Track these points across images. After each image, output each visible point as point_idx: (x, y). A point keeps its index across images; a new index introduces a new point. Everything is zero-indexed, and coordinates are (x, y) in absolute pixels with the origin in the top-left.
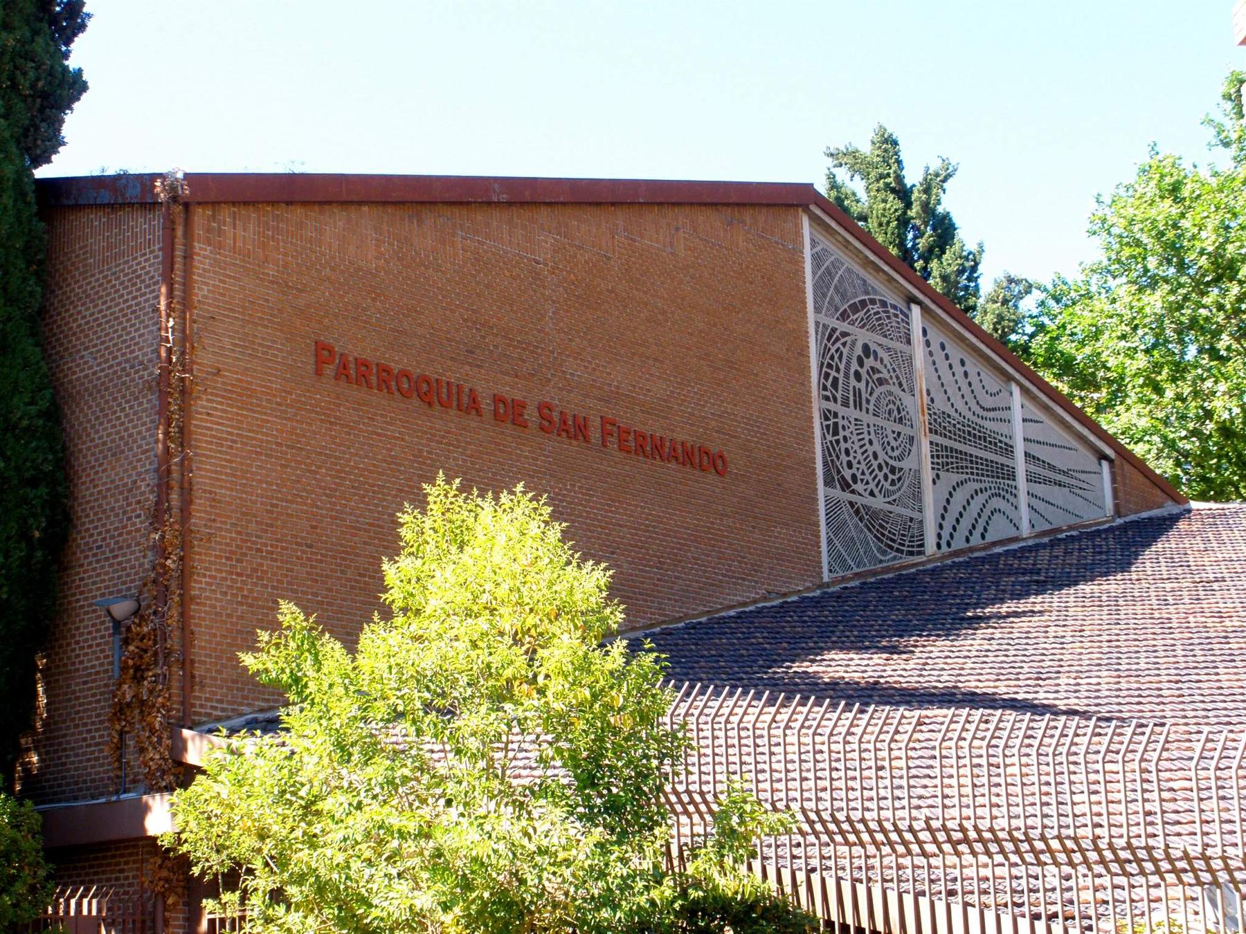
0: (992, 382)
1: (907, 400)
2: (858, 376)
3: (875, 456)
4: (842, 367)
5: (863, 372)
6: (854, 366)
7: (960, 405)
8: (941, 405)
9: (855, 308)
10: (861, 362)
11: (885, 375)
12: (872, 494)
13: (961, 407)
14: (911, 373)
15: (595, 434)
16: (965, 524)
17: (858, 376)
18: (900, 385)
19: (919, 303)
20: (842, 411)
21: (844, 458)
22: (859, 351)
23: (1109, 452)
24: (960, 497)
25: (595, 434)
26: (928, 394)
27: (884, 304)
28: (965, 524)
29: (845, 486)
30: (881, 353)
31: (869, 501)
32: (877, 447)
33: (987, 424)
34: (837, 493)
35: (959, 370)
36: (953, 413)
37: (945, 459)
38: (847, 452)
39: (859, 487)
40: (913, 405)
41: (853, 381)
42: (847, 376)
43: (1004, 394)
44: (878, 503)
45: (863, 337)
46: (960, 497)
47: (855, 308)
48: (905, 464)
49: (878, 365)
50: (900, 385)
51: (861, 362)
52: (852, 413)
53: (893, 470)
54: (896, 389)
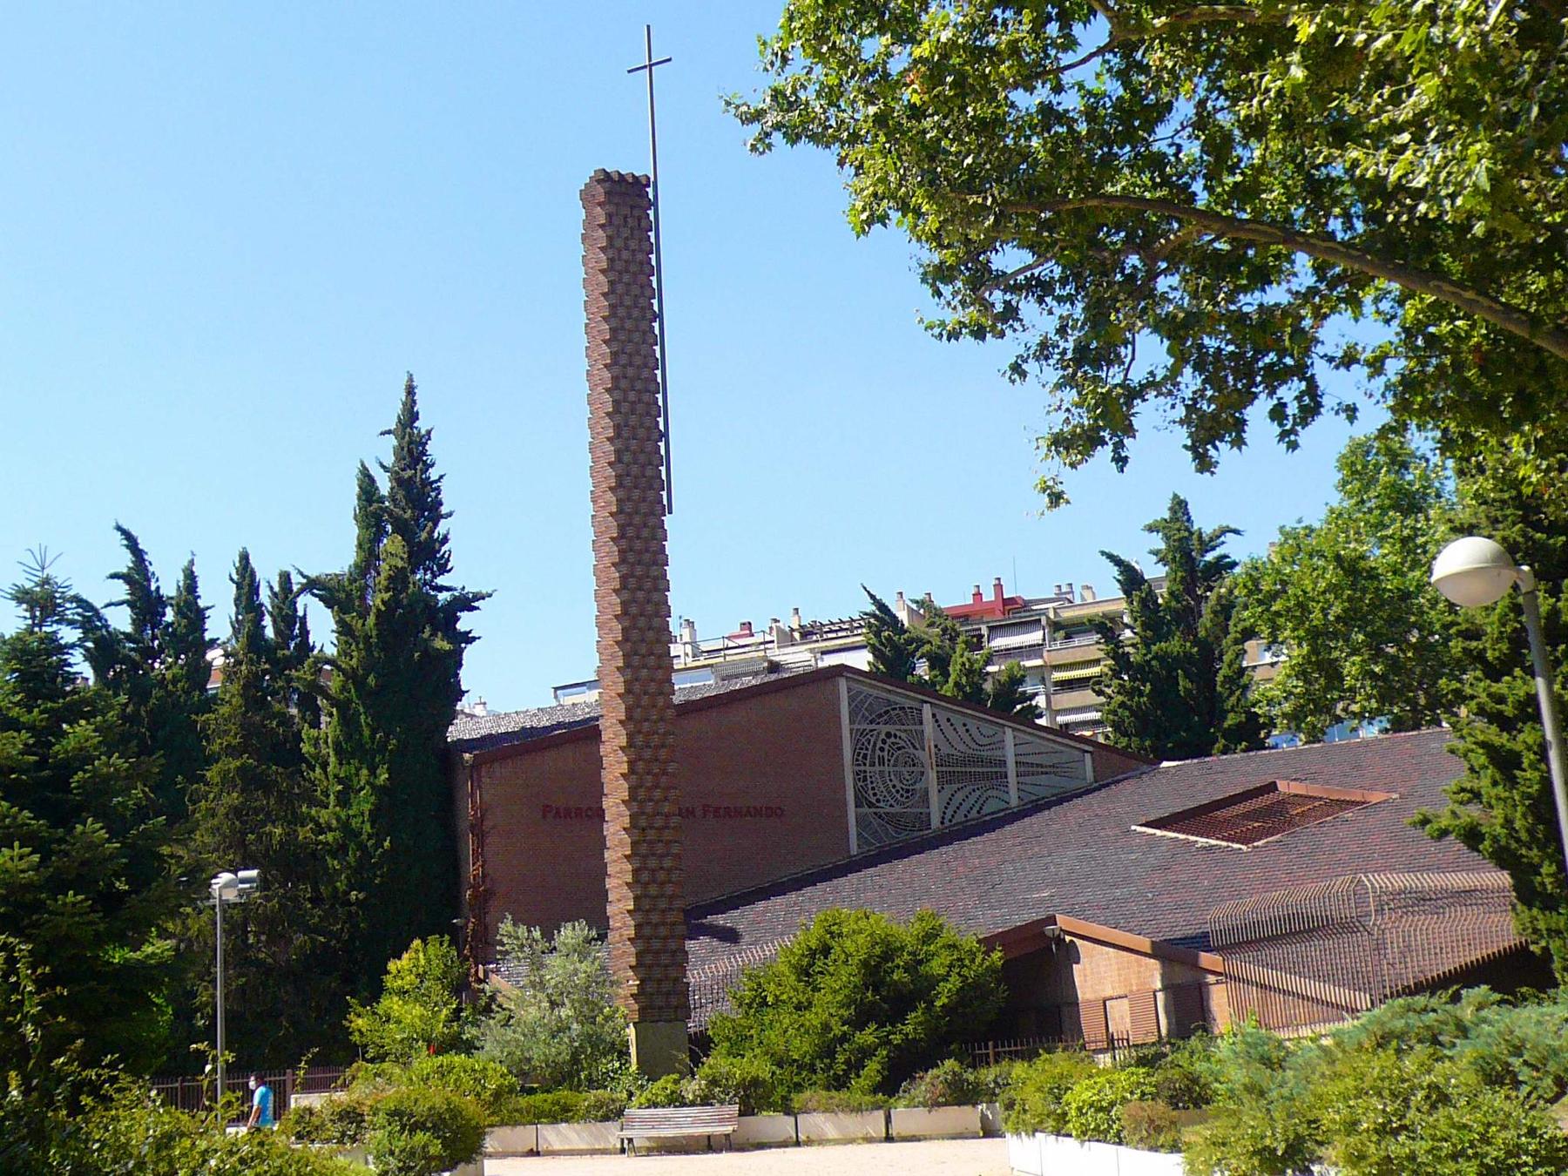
0: (987, 729)
1: (919, 753)
2: (882, 749)
3: (894, 786)
4: (870, 747)
5: (886, 747)
6: (879, 744)
7: (962, 748)
8: (945, 749)
9: (880, 716)
10: (884, 742)
11: (902, 744)
12: (891, 806)
13: (960, 746)
14: (923, 739)
15: (699, 813)
16: (966, 806)
17: (882, 749)
18: (914, 747)
19: (926, 702)
20: (868, 768)
21: (871, 792)
22: (883, 736)
23: (1087, 748)
24: (960, 796)
25: (699, 813)
26: (936, 746)
27: (902, 709)
28: (966, 806)
29: (871, 805)
30: (898, 733)
31: (888, 809)
32: (896, 782)
33: (985, 753)
34: (866, 810)
35: (961, 730)
36: (955, 752)
37: (944, 779)
38: (873, 789)
39: (882, 804)
40: (923, 756)
41: (878, 752)
42: (874, 751)
43: (1001, 734)
44: (897, 809)
45: (885, 729)
46: (960, 796)
47: (880, 716)
48: (917, 786)
49: (898, 740)
50: (914, 747)
51: (884, 742)
52: (877, 768)
53: (908, 791)
54: (912, 750)
